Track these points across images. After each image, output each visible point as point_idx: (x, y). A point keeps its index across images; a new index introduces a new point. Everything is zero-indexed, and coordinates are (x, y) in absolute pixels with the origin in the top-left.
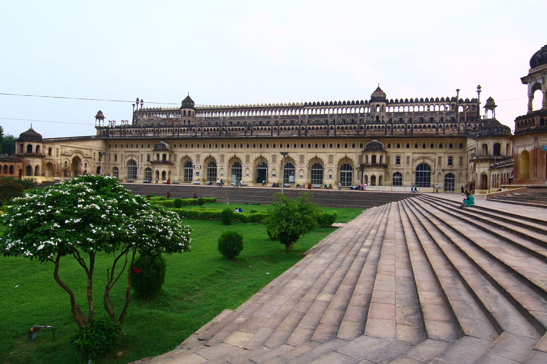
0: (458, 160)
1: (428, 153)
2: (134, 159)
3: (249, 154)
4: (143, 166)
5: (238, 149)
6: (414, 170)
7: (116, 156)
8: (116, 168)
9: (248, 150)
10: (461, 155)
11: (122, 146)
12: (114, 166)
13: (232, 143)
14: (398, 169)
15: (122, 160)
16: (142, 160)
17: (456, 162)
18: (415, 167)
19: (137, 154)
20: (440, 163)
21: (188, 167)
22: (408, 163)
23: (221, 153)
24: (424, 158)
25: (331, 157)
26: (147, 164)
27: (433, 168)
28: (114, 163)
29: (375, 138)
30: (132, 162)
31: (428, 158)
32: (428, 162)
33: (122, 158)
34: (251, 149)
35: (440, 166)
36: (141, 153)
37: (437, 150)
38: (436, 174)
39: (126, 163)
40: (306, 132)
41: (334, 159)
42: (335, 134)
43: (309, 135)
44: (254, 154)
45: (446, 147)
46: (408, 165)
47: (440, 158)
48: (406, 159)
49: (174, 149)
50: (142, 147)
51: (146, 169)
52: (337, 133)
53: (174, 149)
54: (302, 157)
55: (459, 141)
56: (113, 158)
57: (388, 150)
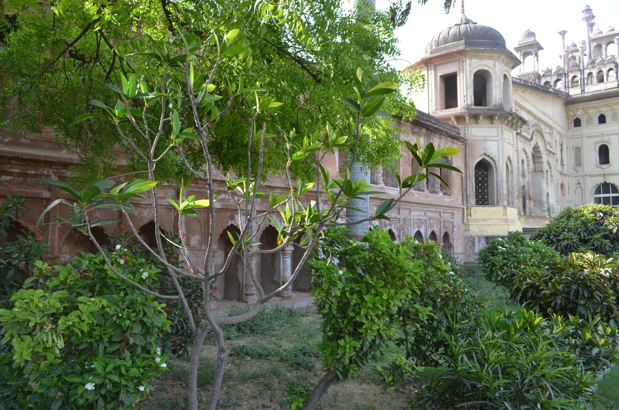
12: (600, 180)
28: (598, 171)
56: (591, 156)
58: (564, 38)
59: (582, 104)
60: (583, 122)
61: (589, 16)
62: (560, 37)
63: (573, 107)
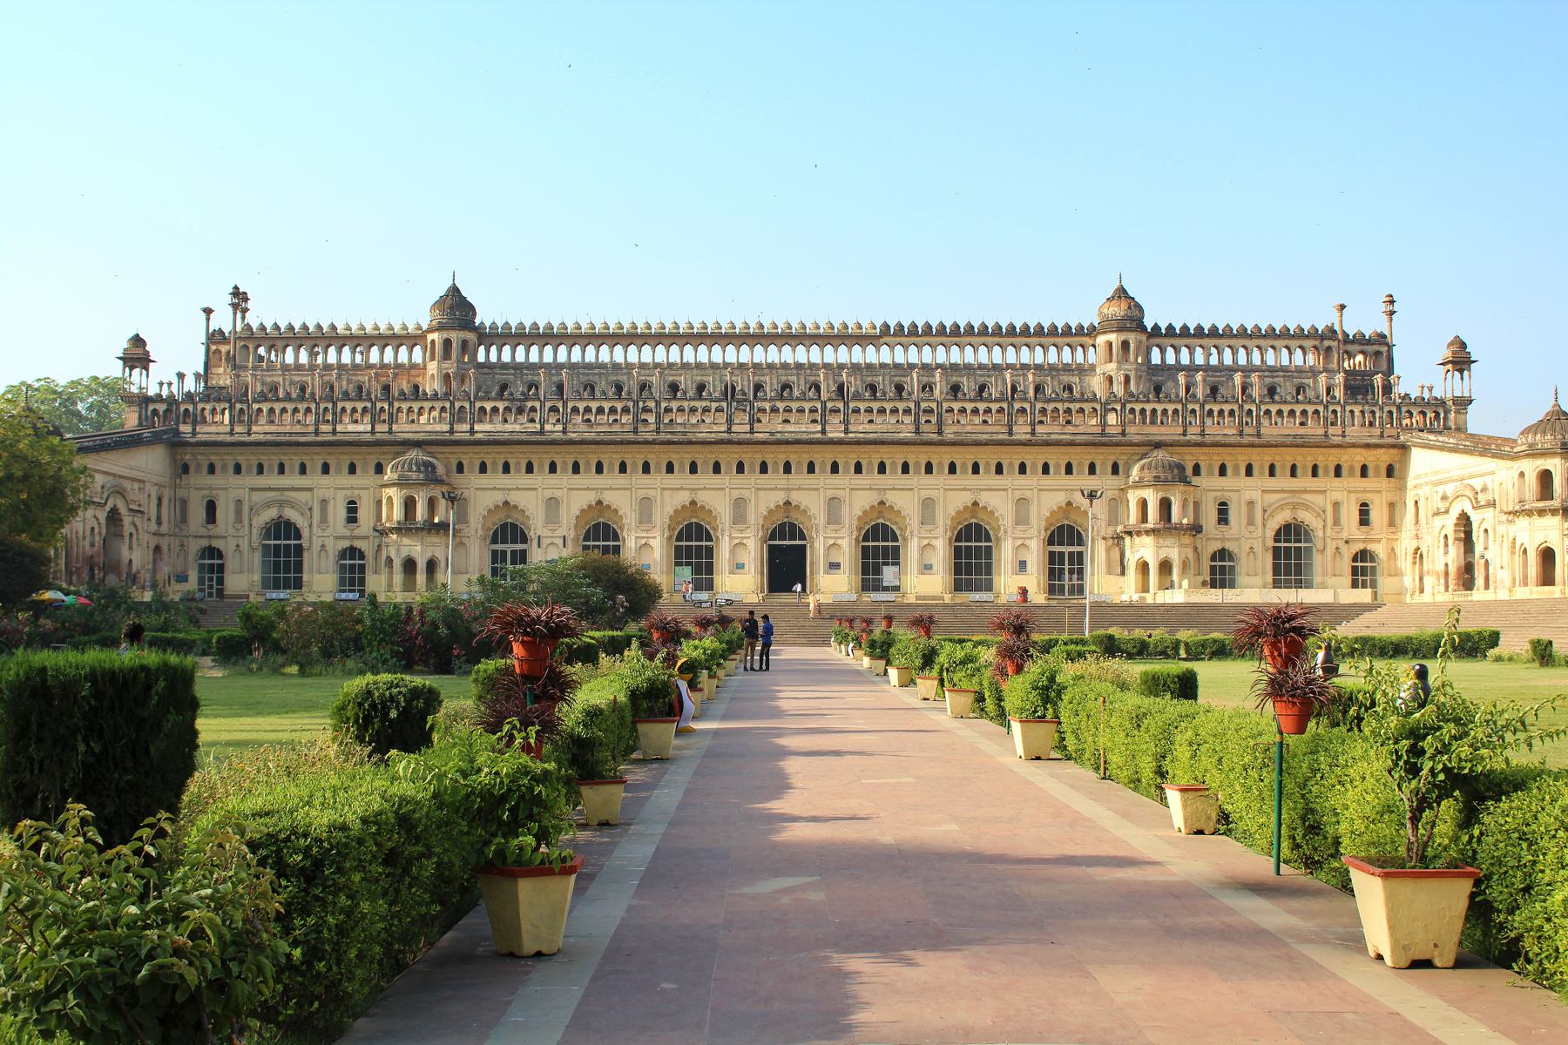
0: (1385, 510)
1: (1306, 491)
2: (292, 515)
3: (746, 493)
4: (329, 543)
5: (705, 478)
6: (1271, 543)
7: (211, 508)
8: (213, 552)
9: (740, 480)
10: (1392, 497)
11: (238, 469)
12: (205, 543)
13: (681, 457)
14: (1223, 540)
15: (239, 519)
16: (324, 519)
17: (1378, 515)
18: (1270, 534)
19: (302, 497)
20: (1337, 522)
21: (504, 541)
22: (1251, 522)
23: (642, 493)
24: (1295, 506)
25: (1022, 503)
26: (348, 533)
27: (1320, 533)
28: (203, 531)
29: (1158, 445)
30: (283, 529)
31: (1307, 507)
32: (1306, 517)
33: (239, 512)
34: (752, 478)
35: (1337, 529)
36: (320, 494)
37: (1326, 481)
38: (1330, 551)
39: (255, 531)
40: (940, 423)
41: (1033, 509)
42: (1033, 433)
43: (949, 433)
44: (765, 496)
45: (1351, 474)
46: (1251, 528)
47: (1336, 505)
48: (1244, 508)
49: (458, 480)
50: (326, 469)
51: (343, 554)
52: (1039, 429)
53: (458, 480)
54: (928, 505)
55: (1384, 457)
56: (197, 513)
57: (1195, 480)
58: (208, 319)
59: (189, 449)
60: (192, 469)
61: (239, 299)
62: (204, 315)
63: (180, 450)
